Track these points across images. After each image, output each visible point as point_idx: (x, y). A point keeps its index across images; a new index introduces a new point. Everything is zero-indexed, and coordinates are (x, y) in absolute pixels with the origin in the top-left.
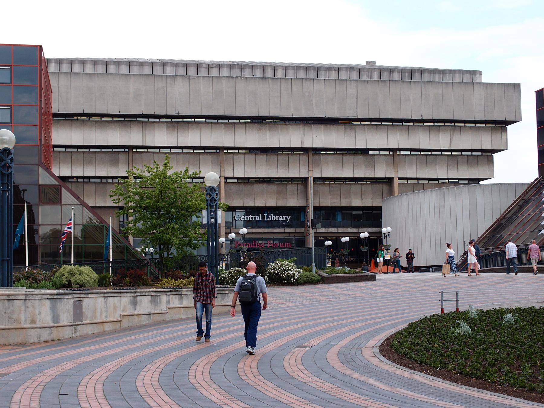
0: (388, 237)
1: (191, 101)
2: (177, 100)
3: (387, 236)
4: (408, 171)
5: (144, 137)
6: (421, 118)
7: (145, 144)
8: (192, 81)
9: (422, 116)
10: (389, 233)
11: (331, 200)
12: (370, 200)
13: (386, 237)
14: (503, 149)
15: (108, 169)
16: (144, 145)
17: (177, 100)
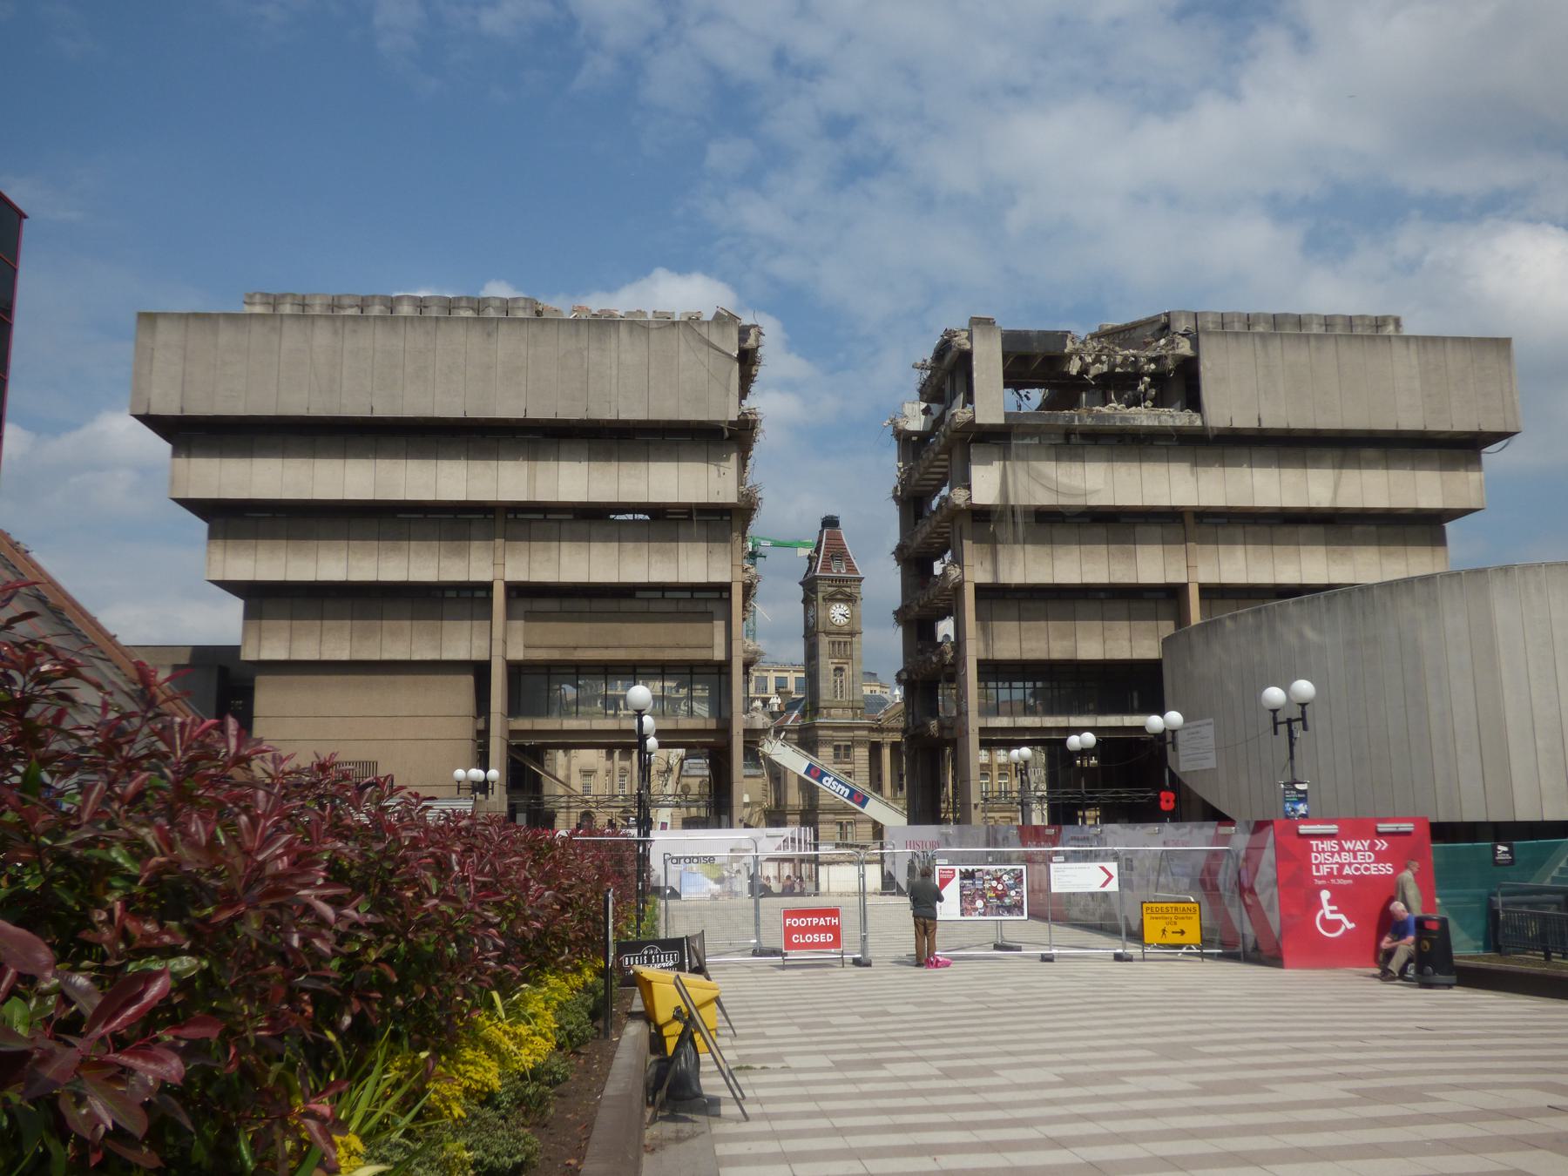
0: (1297, 726)
1: (651, 383)
2: (614, 381)
3: (1289, 722)
4: (1225, 567)
5: (532, 478)
7: (534, 497)
8: (654, 335)
9: (1259, 420)
10: (1303, 705)
12: (1126, 644)
13: (1283, 729)
14: (1473, 506)
15: (441, 565)
16: (532, 499)
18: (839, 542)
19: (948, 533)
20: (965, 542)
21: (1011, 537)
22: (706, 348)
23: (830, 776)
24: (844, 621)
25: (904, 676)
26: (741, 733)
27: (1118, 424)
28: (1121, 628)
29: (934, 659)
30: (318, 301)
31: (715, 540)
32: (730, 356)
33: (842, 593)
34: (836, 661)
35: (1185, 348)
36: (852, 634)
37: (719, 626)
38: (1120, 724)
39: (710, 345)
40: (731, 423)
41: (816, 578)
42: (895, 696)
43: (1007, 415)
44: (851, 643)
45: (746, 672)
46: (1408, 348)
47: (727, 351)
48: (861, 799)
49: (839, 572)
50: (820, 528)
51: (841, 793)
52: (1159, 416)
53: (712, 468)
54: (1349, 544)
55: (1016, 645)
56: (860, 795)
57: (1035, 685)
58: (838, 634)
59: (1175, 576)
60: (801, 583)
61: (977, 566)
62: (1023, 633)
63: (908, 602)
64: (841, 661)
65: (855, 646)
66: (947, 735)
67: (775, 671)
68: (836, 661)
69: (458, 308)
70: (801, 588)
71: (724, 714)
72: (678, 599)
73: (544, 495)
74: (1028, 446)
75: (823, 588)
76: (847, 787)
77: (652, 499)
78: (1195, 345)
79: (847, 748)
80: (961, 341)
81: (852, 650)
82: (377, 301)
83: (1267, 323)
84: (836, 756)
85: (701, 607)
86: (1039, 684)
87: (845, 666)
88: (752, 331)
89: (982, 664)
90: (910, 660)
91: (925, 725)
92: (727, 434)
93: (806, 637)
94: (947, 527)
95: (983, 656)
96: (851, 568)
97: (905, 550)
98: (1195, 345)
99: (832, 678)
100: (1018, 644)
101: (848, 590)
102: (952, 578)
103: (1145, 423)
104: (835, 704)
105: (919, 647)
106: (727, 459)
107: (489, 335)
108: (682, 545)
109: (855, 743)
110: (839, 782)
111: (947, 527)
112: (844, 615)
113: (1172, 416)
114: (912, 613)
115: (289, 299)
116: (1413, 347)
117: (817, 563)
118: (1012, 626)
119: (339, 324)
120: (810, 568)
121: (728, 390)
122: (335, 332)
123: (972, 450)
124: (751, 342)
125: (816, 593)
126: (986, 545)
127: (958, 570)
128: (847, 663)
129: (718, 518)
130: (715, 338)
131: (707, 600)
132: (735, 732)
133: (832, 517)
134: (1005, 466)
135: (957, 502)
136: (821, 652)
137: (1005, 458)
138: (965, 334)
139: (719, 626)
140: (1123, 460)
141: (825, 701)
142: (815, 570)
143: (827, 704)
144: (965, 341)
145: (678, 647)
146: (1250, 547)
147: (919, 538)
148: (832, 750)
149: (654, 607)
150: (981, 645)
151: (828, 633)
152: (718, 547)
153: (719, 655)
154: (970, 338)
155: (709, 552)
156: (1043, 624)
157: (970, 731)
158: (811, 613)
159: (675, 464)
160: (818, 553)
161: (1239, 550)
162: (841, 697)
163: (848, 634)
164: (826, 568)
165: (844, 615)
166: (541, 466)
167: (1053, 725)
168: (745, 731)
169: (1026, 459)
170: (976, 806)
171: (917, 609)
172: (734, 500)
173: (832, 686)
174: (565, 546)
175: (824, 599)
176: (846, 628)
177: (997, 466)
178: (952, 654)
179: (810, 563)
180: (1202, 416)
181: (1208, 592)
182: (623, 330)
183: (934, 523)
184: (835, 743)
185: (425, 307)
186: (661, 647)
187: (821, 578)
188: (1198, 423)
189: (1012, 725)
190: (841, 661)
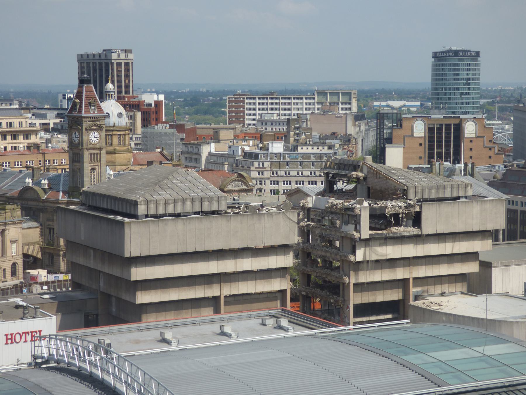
2: (263, 233)
4: (420, 272)
5: (236, 264)
6: (435, 233)
8: (274, 217)
9: (436, 231)
12: (390, 296)
17: (263, 233)
22: (289, 220)
27: (399, 235)
28: (389, 292)
30: (161, 202)
32: (295, 222)
33: (95, 125)
34: (92, 165)
35: (418, 209)
36: (101, 149)
38: (383, 318)
42: (111, 175)
46: (477, 204)
47: (295, 221)
49: (94, 113)
52: (409, 231)
54: (453, 263)
58: (93, 149)
59: (406, 276)
64: (95, 164)
68: (92, 165)
69: (204, 201)
73: (240, 269)
75: (85, 123)
78: (421, 208)
82: (179, 201)
83: (435, 188)
87: (97, 167)
98: (421, 208)
100: (360, 298)
101: (98, 123)
103: (406, 234)
107: (228, 221)
113: (413, 231)
115: (152, 202)
116: (479, 204)
117: (81, 107)
119: (185, 221)
121: (295, 233)
122: (184, 224)
123: (357, 244)
125: (81, 125)
128: (98, 166)
130: (291, 217)
134: (365, 250)
136: (85, 160)
140: (398, 244)
142: (80, 111)
144: (359, 212)
146: (427, 266)
151: (88, 149)
154: (360, 211)
156: (368, 292)
161: (424, 267)
163: (99, 149)
164: (87, 111)
166: (238, 260)
167: (365, 320)
174: (240, 283)
175: (86, 129)
176: (98, 146)
177: (363, 249)
180: (421, 231)
181: (414, 279)
182: (266, 216)
185: (194, 202)
187: (85, 117)
188: (420, 233)
190: (95, 164)
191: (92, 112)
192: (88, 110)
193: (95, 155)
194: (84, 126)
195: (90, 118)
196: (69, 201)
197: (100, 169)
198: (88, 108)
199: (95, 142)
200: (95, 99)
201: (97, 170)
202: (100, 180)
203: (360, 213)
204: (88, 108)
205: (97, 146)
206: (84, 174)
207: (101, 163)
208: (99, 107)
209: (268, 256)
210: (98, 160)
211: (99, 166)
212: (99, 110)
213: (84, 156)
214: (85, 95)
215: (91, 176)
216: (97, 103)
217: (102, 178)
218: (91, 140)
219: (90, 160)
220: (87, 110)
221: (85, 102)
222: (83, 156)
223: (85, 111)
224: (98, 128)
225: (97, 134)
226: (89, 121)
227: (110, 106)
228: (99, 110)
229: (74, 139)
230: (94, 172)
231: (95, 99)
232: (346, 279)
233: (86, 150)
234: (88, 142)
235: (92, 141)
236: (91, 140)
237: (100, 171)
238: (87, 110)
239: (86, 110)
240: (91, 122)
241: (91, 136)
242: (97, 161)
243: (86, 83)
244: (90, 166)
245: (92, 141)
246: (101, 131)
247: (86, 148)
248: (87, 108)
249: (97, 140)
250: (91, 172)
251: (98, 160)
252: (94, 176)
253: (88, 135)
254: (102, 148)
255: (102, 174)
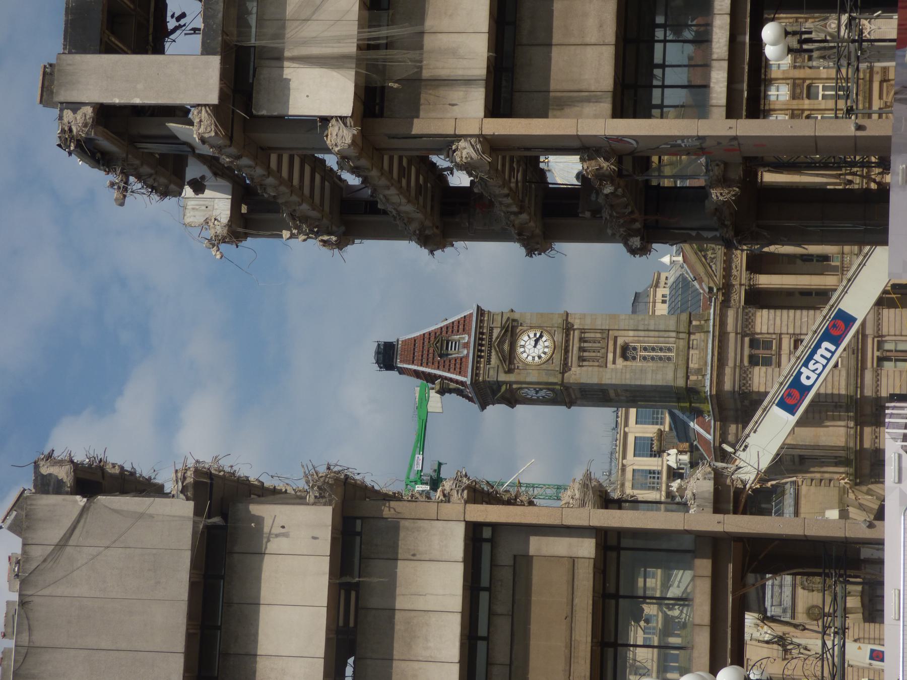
1: (123, 646)
8: (41, 637)
11: (588, 40)
18: (419, 344)
19: (401, 158)
20: (415, 131)
21: (412, 54)
22: (68, 549)
23: (800, 373)
24: (546, 341)
25: (636, 242)
26: (719, 517)
29: (608, 190)
31: (395, 547)
32: (84, 510)
33: (501, 343)
34: (610, 356)
36: (568, 329)
37: (538, 545)
39: (63, 544)
40: (198, 512)
41: (475, 383)
43: (207, 50)
44: (583, 331)
45: (619, 504)
48: (841, 324)
49: (466, 345)
50: (395, 373)
51: (828, 355)
53: (273, 546)
55: (591, 53)
56: (833, 325)
57: (659, 26)
58: (566, 351)
60: (483, 407)
61: (456, 111)
62: (572, 41)
63: (514, 232)
65: (588, 324)
66: (737, 173)
67: (624, 457)
68: (610, 356)
70: (490, 408)
71: (688, 543)
72: (491, 614)
74: (260, 20)
75: (491, 372)
76: (818, 346)
77: (320, 651)
79: (754, 343)
80: (79, 120)
81: (595, 330)
84: (767, 362)
85: (506, 575)
86: (660, 20)
87: (620, 341)
88: (45, 470)
89: (619, 112)
90: (609, 232)
91: (719, 209)
92: (216, 520)
93: (570, 404)
94: (391, 159)
95: (606, 106)
96: (462, 325)
97: (427, 232)
99: (638, 364)
100: (589, 49)
101: (496, 332)
102: (474, 155)
104: (682, 362)
105: (588, 214)
106: (259, 520)
108: (400, 603)
109: (746, 331)
110: (810, 357)
111: (391, 159)
112: (537, 341)
114: (532, 224)
117: (451, 380)
118: (559, 57)
120: (460, 393)
121: (141, 516)
123: (264, 113)
124: (63, 473)
125: (499, 384)
126: (423, 97)
127: (462, 144)
128: (616, 338)
129: (358, 539)
130: (54, 534)
131: (493, 564)
132: (719, 528)
133: (378, 353)
134: (293, 59)
135: (349, 140)
136: (595, 380)
137: (278, 58)
138: (68, 115)
139: (538, 545)
141: (675, 378)
143: (681, 374)
145: (571, 617)
147: (407, 208)
148: (757, 369)
149: (501, 654)
150: (589, 109)
151: (565, 367)
152: (406, 541)
153: (586, 548)
154: (75, 106)
155: (414, 557)
157: (732, 133)
158: (532, 393)
159: (263, 609)
160: (436, 377)
162: (669, 350)
163: (568, 335)
165: (537, 341)
168: (717, 510)
169: (282, 23)
170: (859, 128)
171: (524, 217)
172: (328, 510)
173: (651, 364)
175: (510, 371)
176: (559, 337)
177: (294, 73)
178: (601, 160)
179: (450, 391)
183: (383, 182)
184: (746, 363)
186: (570, 645)
187: (475, 375)
189: (725, 64)
191: (465, 352)
192: (458, 361)
193: (586, 345)
194: (500, 379)
195: (481, 357)
196: (718, 418)
197: (625, 333)
198: (453, 362)
199: (547, 344)
200: (432, 339)
201: (627, 340)
202: (656, 334)
203: (89, 110)
204: (453, 362)
205: (560, 340)
206: (633, 383)
207: (609, 330)
208: (455, 328)
209: (256, 655)
210: (599, 335)
211: (616, 333)
212: (461, 327)
213: (582, 381)
214: (421, 365)
215: (645, 358)
216: (444, 330)
217: (652, 328)
218: (540, 357)
219: (596, 364)
220: (458, 366)
221: (438, 368)
222: (583, 383)
223: (460, 374)
224: (509, 334)
225: (526, 338)
226: (489, 362)
227: (561, 165)
228: (461, 327)
229: (543, 397)
230: (635, 349)
231: (432, 339)
232: (464, 155)
233: (566, 375)
234: (544, 366)
235: (545, 353)
236: (540, 357)
237: (631, 333)
238: (458, 366)
239: (458, 370)
240: (493, 353)
241: (530, 358)
242: (604, 339)
243: (393, 362)
244: (614, 362)
245: (543, 355)
246: (517, 327)
247: (560, 376)
248: (452, 366)
249: (544, 339)
250: (634, 358)
251: (599, 335)
252: (645, 349)
253: (527, 366)
254: (568, 323)
255: (641, 328)
